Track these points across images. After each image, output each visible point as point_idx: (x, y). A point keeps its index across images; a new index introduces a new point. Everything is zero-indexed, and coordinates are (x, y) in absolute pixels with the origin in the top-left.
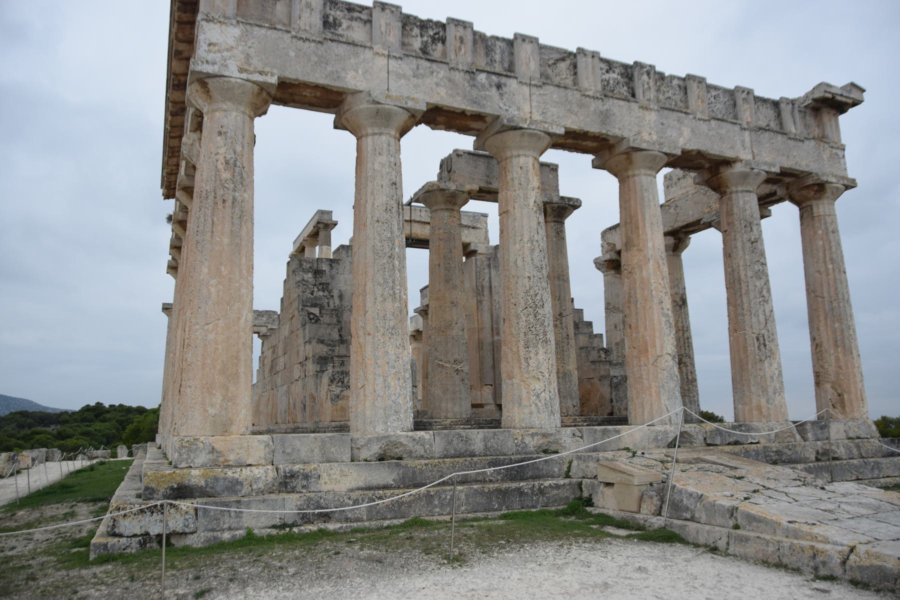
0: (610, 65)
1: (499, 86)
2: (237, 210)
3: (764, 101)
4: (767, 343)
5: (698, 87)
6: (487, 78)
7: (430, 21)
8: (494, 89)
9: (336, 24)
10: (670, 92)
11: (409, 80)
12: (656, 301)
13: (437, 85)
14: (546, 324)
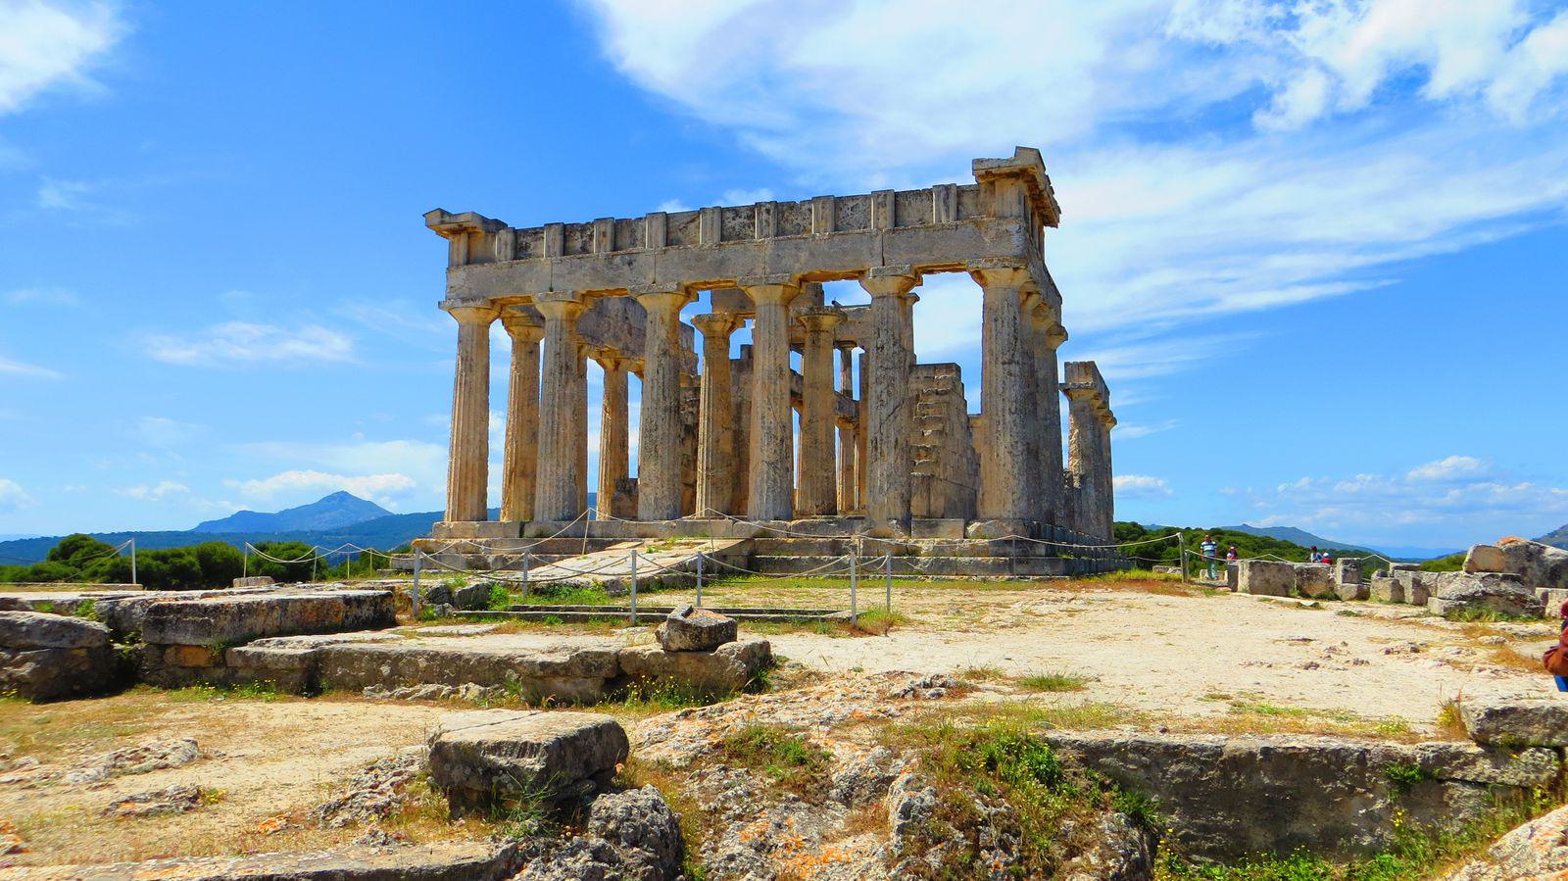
0: (736, 211)
1: (630, 263)
2: (467, 388)
3: (917, 193)
4: (879, 445)
5: (823, 208)
6: (621, 260)
7: (588, 223)
8: (626, 267)
9: (527, 247)
10: (799, 218)
11: (564, 277)
12: (760, 415)
13: (584, 275)
14: (658, 443)
